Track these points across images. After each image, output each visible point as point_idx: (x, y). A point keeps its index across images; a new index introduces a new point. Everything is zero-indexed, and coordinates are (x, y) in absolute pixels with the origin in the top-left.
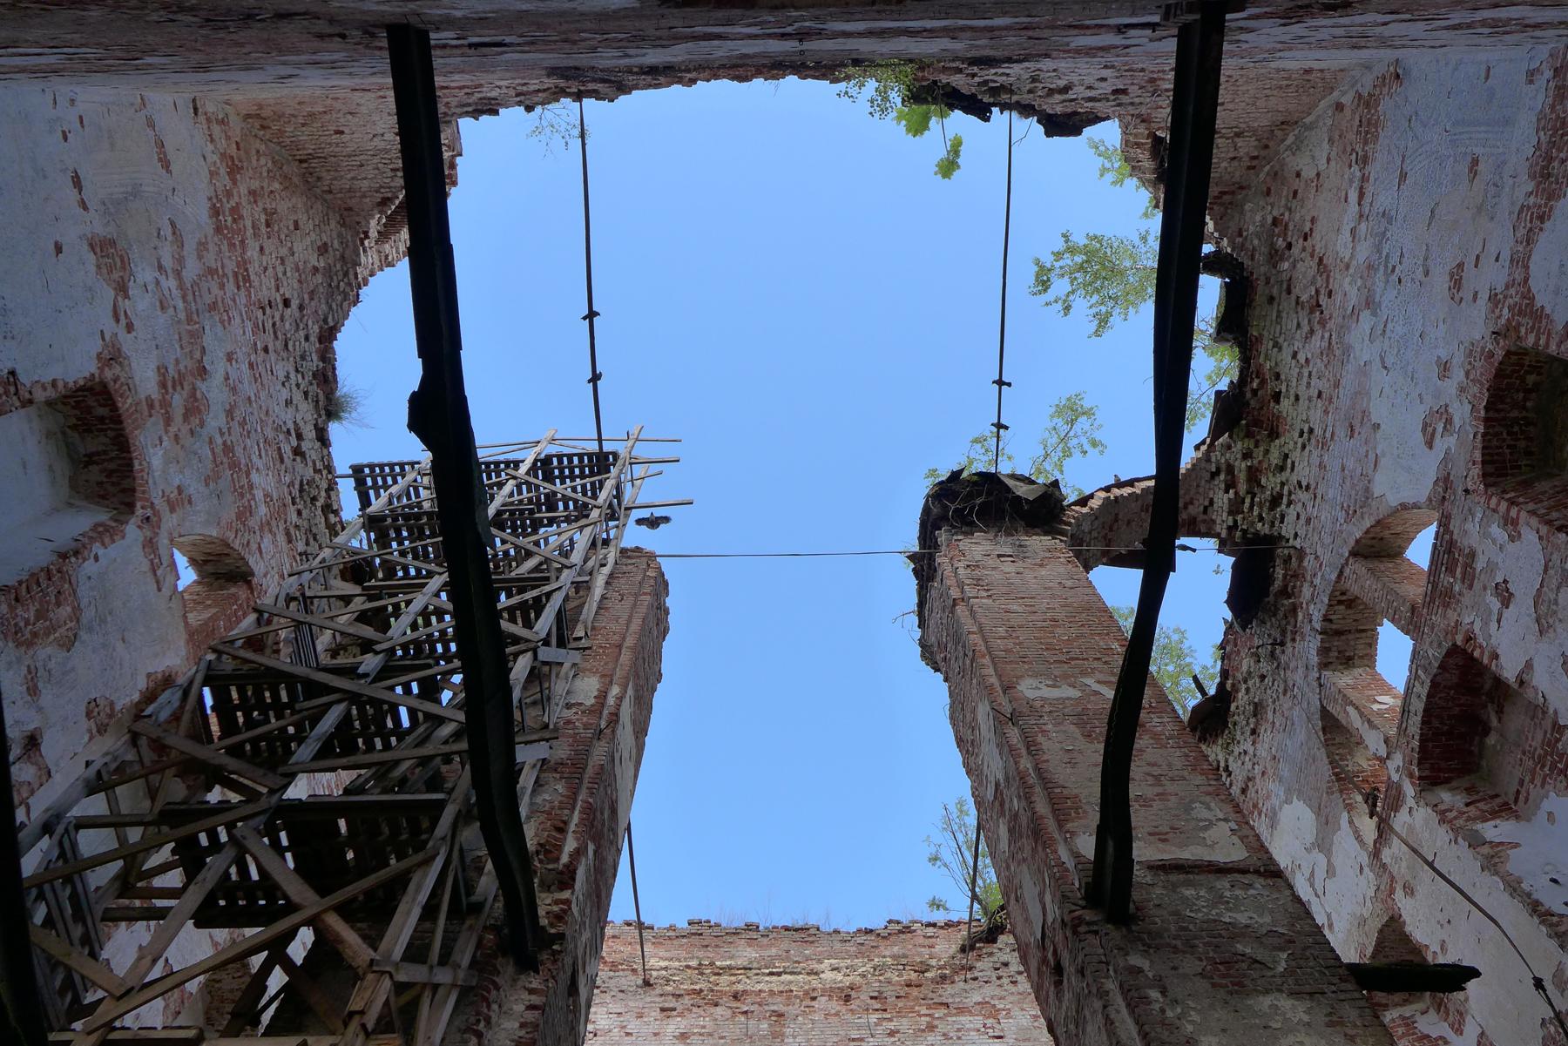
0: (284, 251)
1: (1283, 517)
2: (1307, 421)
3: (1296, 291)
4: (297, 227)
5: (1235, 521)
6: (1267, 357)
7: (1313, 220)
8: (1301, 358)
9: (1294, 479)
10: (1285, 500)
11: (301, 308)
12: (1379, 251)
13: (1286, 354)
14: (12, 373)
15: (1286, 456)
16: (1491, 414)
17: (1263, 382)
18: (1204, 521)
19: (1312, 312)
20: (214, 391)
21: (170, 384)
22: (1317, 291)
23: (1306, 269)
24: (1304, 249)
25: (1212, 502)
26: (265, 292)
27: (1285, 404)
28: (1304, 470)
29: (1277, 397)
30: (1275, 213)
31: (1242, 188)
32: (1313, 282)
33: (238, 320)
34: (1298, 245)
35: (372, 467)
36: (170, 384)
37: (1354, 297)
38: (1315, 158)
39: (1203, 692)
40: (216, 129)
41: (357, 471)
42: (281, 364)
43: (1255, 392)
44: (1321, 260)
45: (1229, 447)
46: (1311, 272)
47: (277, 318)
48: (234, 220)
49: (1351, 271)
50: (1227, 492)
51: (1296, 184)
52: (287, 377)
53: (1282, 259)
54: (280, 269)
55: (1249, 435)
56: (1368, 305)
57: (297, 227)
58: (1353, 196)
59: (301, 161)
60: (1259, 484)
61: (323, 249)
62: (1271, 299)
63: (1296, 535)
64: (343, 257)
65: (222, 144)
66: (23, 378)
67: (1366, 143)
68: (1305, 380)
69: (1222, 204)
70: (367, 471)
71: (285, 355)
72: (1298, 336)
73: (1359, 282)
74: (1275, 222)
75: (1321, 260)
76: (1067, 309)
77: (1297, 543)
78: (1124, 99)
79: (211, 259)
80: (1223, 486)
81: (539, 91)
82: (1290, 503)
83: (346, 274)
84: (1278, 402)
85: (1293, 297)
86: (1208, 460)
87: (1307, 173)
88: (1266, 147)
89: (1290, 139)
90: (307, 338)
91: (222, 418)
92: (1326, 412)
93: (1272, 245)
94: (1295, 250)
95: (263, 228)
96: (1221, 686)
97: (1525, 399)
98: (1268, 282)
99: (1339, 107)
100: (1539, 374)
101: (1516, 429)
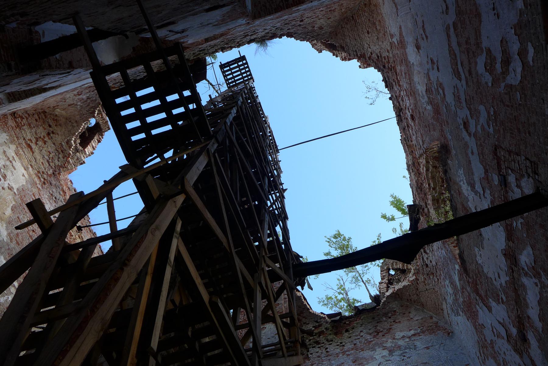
0: (320, 17)
1: (314, 347)
2: (346, 343)
3: (379, 324)
4: (328, 19)
6: (357, 324)
7: (400, 322)
8: (362, 334)
9: (327, 346)
10: (319, 346)
11: (300, 25)
12: (406, 348)
13: (361, 329)
15: (332, 341)
17: (349, 325)
19: (376, 332)
22: (382, 331)
23: (386, 325)
25: (307, 324)
27: (346, 334)
28: (333, 349)
29: (347, 331)
30: (397, 310)
32: (384, 329)
35: (247, 63)
37: (389, 345)
38: (416, 316)
41: (243, 58)
43: (345, 323)
44: (391, 329)
45: (327, 323)
46: (386, 327)
49: (394, 341)
50: (313, 327)
53: (385, 317)
54: (314, 17)
55: (333, 327)
56: (390, 351)
57: (328, 19)
58: (412, 332)
59: (353, 17)
60: (319, 336)
61: (321, 28)
62: (374, 318)
63: (311, 354)
64: (319, 35)
67: (428, 330)
68: (356, 338)
70: (244, 62)
73: (393, 345)
74: (395, 311)
75: (391, 329)
77: (310, 356)
78: (424, 267)
82: (319, 348)
83: (313, 37)
85: (377, 324)
86: (320, 319)
87: (411, 315)
90: (288, 29)
92: (352, 349)
93: (388, 313)
94: (389, 320)
99: (431, 318)
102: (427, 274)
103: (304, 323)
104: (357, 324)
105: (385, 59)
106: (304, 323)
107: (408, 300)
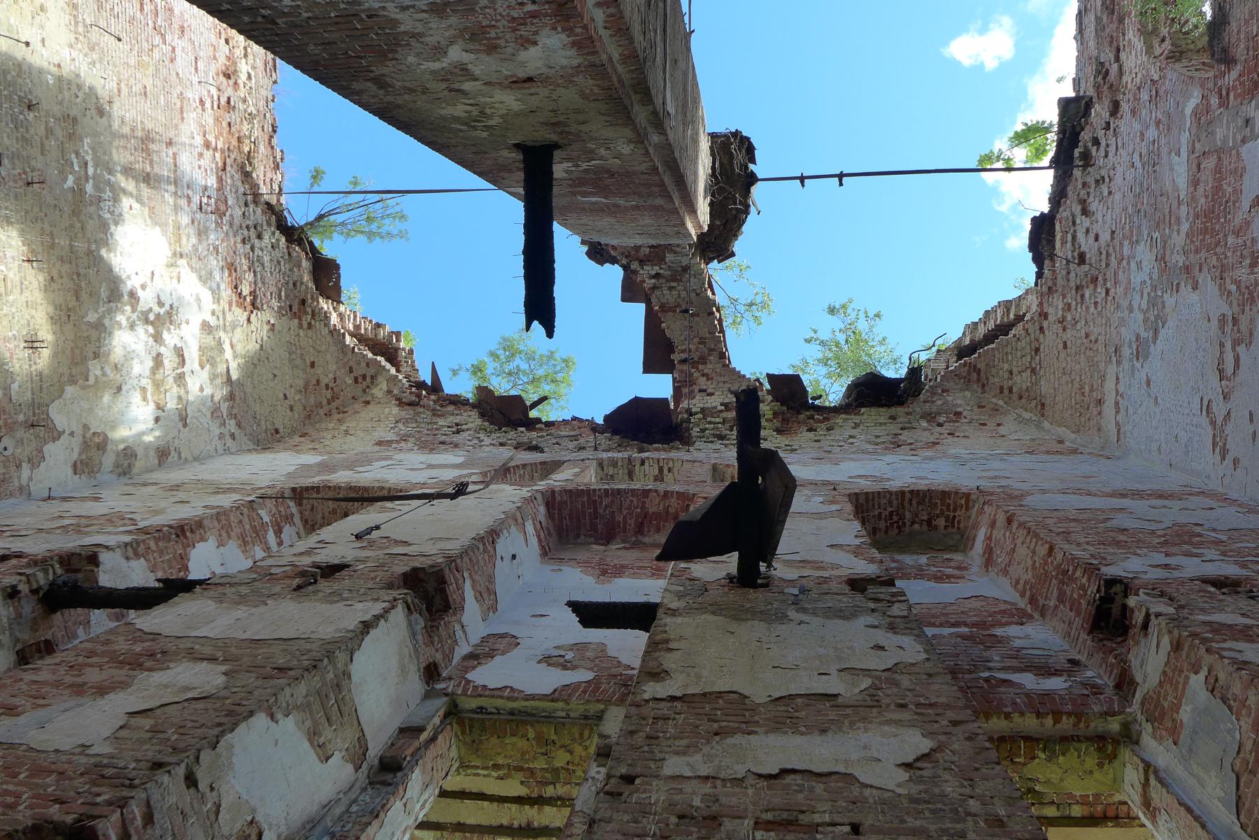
3: (905, 432)
5: (696, 413)
8: (851, 440)
13: (854, 432)
16: (908, 496)
18: (693, 391)
25: (711, 394)
27: (811, 435)
30: (965, 413)
31: (983, 386)
39: (535, 405)
51: (991, 424)
55: (775, 414)
62: (893, 418)
74: (958, 414)
76: (808, 341)
80: (727, 401)
87: (1002, 430)
89: (1027, 415)
93: (939, 414)
96: (538, 420)
97: (921, 523)
98: (907, 414)
100: (946, 527)
101: (895, 518)
106: (701, 391)
107: (1002, 388)
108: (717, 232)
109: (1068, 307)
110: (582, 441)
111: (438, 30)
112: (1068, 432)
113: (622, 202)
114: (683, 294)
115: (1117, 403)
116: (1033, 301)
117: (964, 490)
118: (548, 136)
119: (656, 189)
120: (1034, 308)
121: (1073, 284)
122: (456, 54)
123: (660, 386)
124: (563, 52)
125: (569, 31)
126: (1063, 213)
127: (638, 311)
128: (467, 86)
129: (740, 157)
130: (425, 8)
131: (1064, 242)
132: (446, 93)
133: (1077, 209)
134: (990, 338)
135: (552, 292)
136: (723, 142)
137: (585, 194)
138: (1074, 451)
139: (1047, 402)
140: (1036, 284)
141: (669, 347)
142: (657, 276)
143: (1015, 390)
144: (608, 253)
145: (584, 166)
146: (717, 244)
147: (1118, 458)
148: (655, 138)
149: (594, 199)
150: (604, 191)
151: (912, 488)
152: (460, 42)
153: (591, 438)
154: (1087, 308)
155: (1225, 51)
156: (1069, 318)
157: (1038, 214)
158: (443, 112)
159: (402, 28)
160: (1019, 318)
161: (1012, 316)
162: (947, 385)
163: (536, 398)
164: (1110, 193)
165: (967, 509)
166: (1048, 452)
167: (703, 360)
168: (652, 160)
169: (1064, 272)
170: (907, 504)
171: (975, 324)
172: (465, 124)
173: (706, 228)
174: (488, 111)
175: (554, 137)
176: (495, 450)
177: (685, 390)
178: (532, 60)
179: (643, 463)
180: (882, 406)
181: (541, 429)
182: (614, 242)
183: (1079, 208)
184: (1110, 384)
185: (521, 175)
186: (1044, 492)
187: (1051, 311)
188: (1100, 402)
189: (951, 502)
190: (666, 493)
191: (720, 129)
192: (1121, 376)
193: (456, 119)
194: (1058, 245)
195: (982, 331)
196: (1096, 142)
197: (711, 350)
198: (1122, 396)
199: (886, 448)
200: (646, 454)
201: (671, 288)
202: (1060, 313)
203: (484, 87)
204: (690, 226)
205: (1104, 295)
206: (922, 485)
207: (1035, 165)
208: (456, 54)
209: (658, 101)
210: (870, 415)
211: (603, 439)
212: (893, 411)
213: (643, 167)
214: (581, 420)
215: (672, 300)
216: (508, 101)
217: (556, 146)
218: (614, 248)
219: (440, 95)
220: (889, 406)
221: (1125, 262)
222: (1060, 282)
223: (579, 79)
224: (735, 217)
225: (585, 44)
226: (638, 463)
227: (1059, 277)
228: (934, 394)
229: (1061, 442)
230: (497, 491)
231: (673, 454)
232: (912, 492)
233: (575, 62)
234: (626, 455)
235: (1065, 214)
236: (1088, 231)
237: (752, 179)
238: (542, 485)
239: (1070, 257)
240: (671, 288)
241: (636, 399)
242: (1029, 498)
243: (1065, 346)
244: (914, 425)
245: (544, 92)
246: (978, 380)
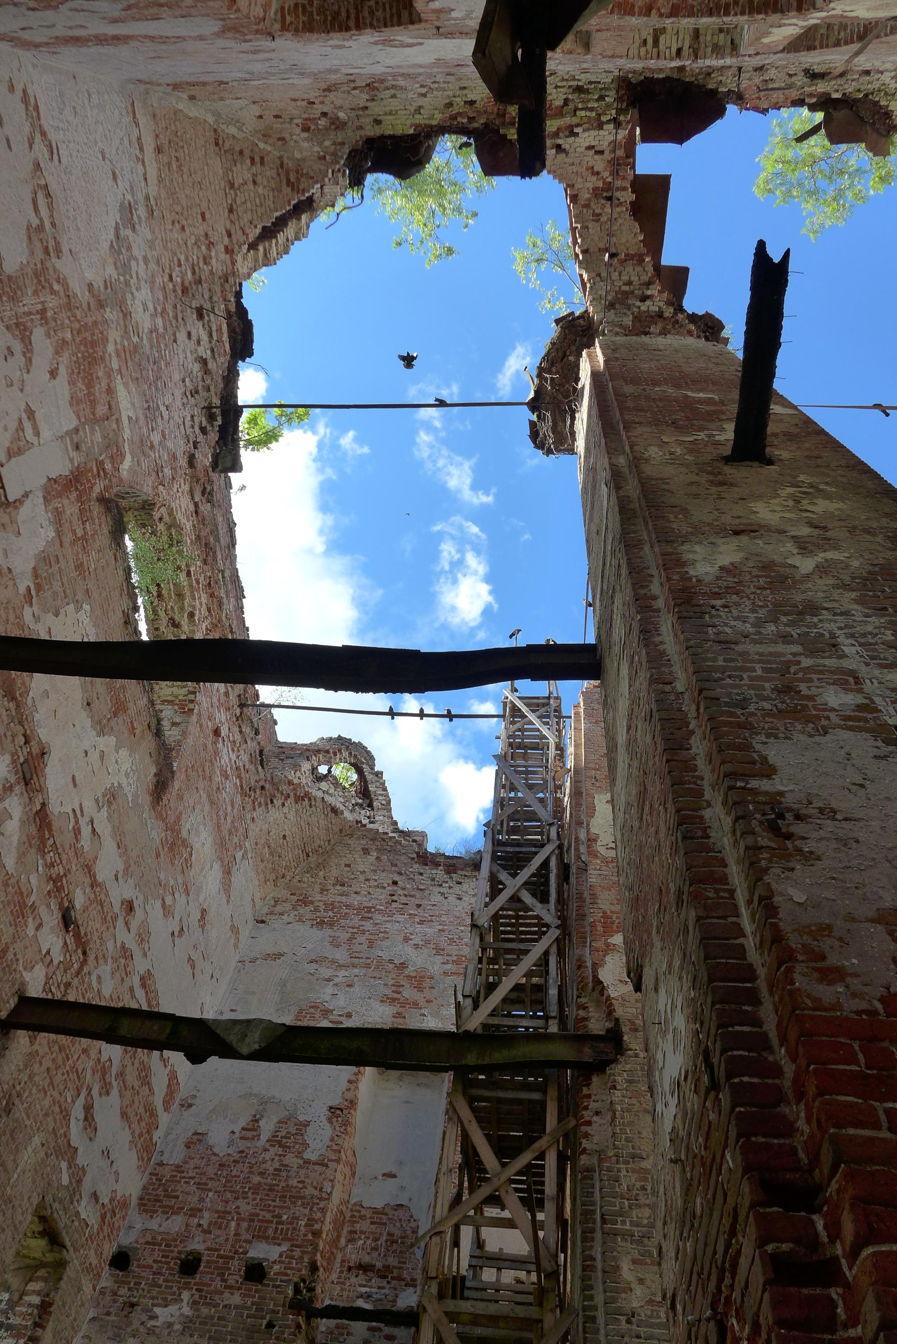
3: (362, 104)
5: (608, 122)
6: (432, 117)
7: (295, 100)
8: (424, 90)
11: (400, 874)
14: (331, 1108)
16: (352, 24)
20: (418, 960)
21: (396, 996)
24: (322, 103)
25: (590, 148)
26: (383, 897)
27: (471, 97)
30: (298, 130)
31: (282, 165)
33: (389, 925)
34: (319, 108)
36: (396, 996)
40: (279, 909)
42: (432, 897)
47: (401, 892)
48: (332, 910)
50: (577, 135)
51: (269, 117)
52: (442, 894)
53: (338, 118)
54: (373, 883)
59: (308, 856)
61: (366, 851)
62: (378, 122)
65: (288, 906)
66: (335, 1103)
69: (298, 180)
71: (427, 892)
72: (404, 96)
74: (306, 129)
75: (324, 90)
79: (344, 936)
81: (241, 732)
83: (384, 840)
84: (475, 102)
85: (368, 104)
87: (256, 110)
88: (241, 152)
89: (232, 130)
90: (421, 874)
91: (439, 959)
93: (327, 129)
95: (345, 889)
96: (813, 108)
102: (199, 282)
103: (601, 152)
104: (432, 117)
105: (260, 804)
106: (601, 152)
107: (262, 163)
108: (574, 348)
109: (206, 260)
110: (757, 80)
111: (818, 590)
112: (186, 111)
113: (670, 391)
114: (615, 276)
115: (142, 150)
116: (242, 267)
117: (288, 35)
118: (733, 471)
119: (630, 404)
120: (239, 258)
121: (205, 285)
122: (806, 565)
123: (652, 158)
124: (696, 557)
125: (685, 577)
126: (224, 361)
127: (668, 259)
128: (805, 531)
129: (545, 429)
130: (824, 612)
131: (219, 330)
132: (830, 526)
133: (211, 365)
134: (281, 223)
135: (752, 297)
136: (562, 444)
137: (709, 402)
138: (176, 87)
139: (212, 147)
140: (241, 285)
141: (636, 210)
142: (644, 299)
143: (248, 161)
144: (698, 327)
145: (702, 435)
146: (575, 333)
147: (129, 81)
148: (622, 461)
149: (701, 395)
150: (688, 404)
151: (348, 34)
152: (798, 577)
153: (743, 86)
154: (187, 260)
155: (108, 510)
156: (203, 248)
157: (248, 360)
158: (841, 505)
159: (853, 595)
160: (253, 246)
161: (261, 248)
162: (318, 166)
163: (812, 140)
164: (184, 381)
165: (283, 8)
166: (204, 84)
167: (597, 193)
168: (628, 438)
169: (215, 299)
170: (353, 12)
171: (297, 238)
172: (820, 490)
173: (584, 353)
174: (791, 503)
175: (728, 470)
176: (878, 64)
177: (621, 153)
178: (729, 553)
179: (679, 51)
180: (390, 137)
181: (811, 95)
182: (690, 340)
183: (210, 366)
184: (152, 173)
185: (771, 428)
186: (201, 38)
187: (223, 256)
188: (159, 150)
189: (303, 18)
190: (648, 14)
191: (564, 458)
192: (143, 183)
193: (829, 497)
194: (225, 328)
195: (290, 230)
196: (203, 430)
197: (587, 206)
198: (138, 158)
199: (382, 81)
200: (674, 64)
201: (629, 283)
202: (213, 254)
203: (788, 529)
204: (601, 359)
205: (174, 275)
206: (336, 39)
207: (258, 410)
208: (806, 565)
209: (614, 499)
210: (401, 124)
211: (728, 83)
212: (376, 132)
213: (640, 430)
214: (756, 109)
215: (629, 269)
216: (765, 512)
217: (728, 460)
218: (690, 333)
219: (837, 524)
220: (383, 137)
221: (159, 310)
222: (217, 289)
223: (686, 529)
224: (552, 364)
225: (673, 563)
226: (686, 52)
227: (219, 293)
228: (334, 154)
229: (192, 98)
230: (876, 8)
231: (639, 65)
232: (348, 29)
233: (685, 547)
234: (701, 63)
235: (222, 359)
236: (199, 342)
237: (534, 405)
238: (814, 18)
239: (212, 315)
240: (629, 283)
241: (680, 140)
242: (216, 29)
243: (203, 215)
244: (353, 114)
245: (727, 519)
246: (287, 173)
